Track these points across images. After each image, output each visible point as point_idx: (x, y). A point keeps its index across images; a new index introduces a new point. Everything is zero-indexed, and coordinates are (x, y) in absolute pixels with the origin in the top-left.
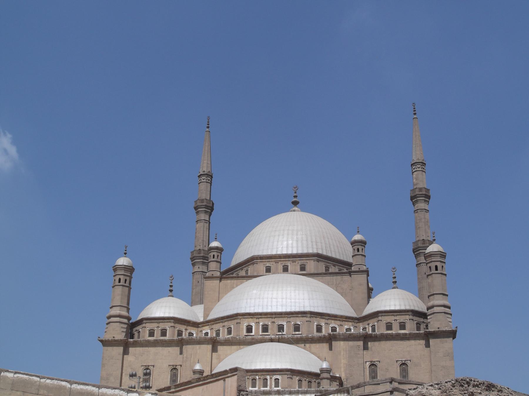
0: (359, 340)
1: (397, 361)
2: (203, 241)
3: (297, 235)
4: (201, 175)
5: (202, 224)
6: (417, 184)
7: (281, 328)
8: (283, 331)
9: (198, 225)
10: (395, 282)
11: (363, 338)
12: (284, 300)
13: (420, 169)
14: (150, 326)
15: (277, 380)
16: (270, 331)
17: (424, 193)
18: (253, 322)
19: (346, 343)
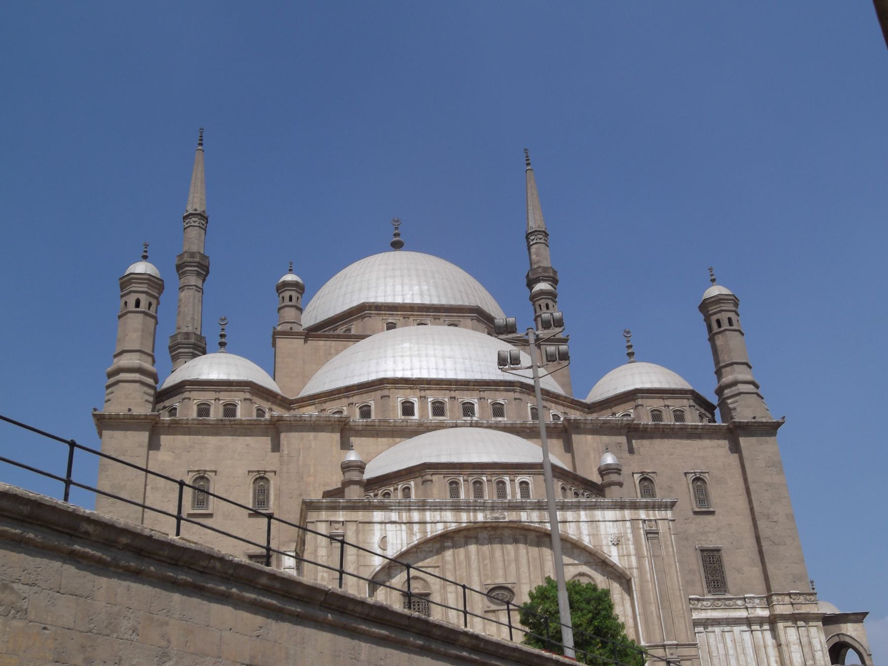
0: (620, 434)
1: (686, 474)
2: (193, 319)
3: (434, 278)
4: (190, 214)
5: (192, 292)
6: (538, 262)
7: (468, 410)
8: (473, 414)
9: (183, 294)
10: (631, 355)
11: (626, 431)
12: (467, 362)
13: (542, 241)
14: (198, 397)
15: (524, 484)
16: (448, 413)
17: (551, 274)
18: (414, 396)
19: (597, 438)
